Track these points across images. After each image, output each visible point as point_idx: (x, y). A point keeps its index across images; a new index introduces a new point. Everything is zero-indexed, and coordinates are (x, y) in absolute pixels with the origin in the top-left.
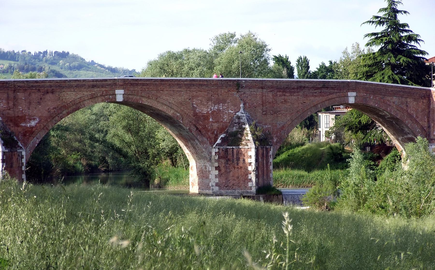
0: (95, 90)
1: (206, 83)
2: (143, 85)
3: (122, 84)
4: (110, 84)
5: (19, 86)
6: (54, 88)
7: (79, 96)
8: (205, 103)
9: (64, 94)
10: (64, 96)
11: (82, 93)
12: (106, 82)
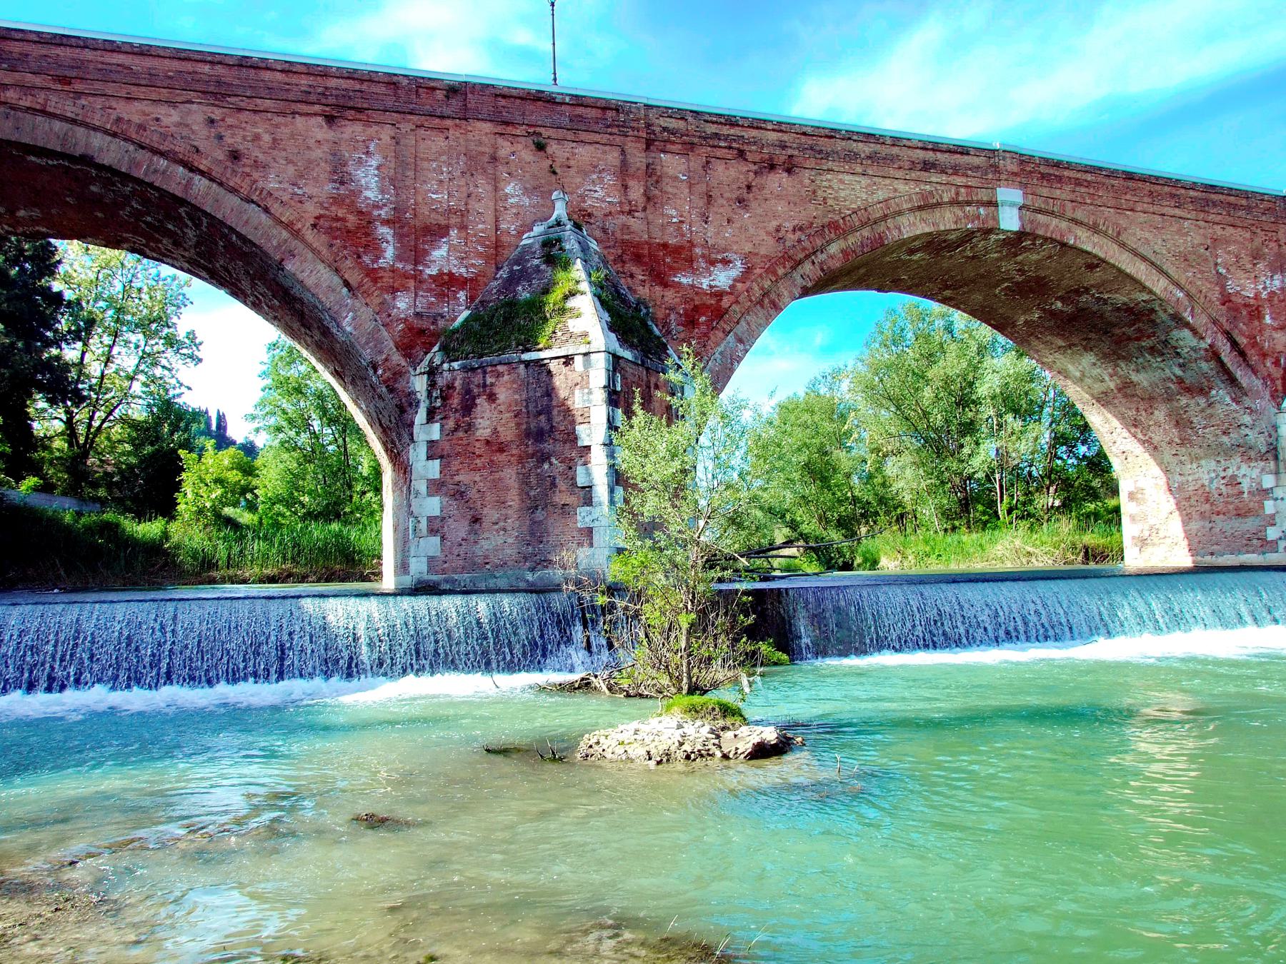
0: (933, 179)
1: (1244, 202)
2: (1078, 182)
3: (1015, 168)
4: (978, 167)
5: (665, 129)
6: (796, 153)
7: (881, 195)
8: (1249, 266)
9: (830, 180)
10: (830, 187)
11: (890, 185)
12: (966, 157)
